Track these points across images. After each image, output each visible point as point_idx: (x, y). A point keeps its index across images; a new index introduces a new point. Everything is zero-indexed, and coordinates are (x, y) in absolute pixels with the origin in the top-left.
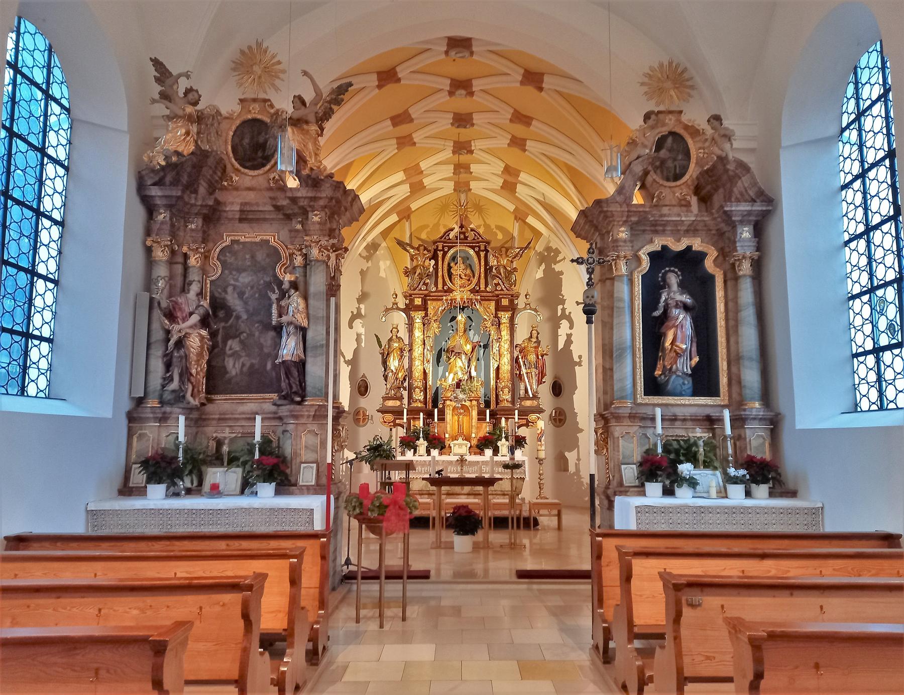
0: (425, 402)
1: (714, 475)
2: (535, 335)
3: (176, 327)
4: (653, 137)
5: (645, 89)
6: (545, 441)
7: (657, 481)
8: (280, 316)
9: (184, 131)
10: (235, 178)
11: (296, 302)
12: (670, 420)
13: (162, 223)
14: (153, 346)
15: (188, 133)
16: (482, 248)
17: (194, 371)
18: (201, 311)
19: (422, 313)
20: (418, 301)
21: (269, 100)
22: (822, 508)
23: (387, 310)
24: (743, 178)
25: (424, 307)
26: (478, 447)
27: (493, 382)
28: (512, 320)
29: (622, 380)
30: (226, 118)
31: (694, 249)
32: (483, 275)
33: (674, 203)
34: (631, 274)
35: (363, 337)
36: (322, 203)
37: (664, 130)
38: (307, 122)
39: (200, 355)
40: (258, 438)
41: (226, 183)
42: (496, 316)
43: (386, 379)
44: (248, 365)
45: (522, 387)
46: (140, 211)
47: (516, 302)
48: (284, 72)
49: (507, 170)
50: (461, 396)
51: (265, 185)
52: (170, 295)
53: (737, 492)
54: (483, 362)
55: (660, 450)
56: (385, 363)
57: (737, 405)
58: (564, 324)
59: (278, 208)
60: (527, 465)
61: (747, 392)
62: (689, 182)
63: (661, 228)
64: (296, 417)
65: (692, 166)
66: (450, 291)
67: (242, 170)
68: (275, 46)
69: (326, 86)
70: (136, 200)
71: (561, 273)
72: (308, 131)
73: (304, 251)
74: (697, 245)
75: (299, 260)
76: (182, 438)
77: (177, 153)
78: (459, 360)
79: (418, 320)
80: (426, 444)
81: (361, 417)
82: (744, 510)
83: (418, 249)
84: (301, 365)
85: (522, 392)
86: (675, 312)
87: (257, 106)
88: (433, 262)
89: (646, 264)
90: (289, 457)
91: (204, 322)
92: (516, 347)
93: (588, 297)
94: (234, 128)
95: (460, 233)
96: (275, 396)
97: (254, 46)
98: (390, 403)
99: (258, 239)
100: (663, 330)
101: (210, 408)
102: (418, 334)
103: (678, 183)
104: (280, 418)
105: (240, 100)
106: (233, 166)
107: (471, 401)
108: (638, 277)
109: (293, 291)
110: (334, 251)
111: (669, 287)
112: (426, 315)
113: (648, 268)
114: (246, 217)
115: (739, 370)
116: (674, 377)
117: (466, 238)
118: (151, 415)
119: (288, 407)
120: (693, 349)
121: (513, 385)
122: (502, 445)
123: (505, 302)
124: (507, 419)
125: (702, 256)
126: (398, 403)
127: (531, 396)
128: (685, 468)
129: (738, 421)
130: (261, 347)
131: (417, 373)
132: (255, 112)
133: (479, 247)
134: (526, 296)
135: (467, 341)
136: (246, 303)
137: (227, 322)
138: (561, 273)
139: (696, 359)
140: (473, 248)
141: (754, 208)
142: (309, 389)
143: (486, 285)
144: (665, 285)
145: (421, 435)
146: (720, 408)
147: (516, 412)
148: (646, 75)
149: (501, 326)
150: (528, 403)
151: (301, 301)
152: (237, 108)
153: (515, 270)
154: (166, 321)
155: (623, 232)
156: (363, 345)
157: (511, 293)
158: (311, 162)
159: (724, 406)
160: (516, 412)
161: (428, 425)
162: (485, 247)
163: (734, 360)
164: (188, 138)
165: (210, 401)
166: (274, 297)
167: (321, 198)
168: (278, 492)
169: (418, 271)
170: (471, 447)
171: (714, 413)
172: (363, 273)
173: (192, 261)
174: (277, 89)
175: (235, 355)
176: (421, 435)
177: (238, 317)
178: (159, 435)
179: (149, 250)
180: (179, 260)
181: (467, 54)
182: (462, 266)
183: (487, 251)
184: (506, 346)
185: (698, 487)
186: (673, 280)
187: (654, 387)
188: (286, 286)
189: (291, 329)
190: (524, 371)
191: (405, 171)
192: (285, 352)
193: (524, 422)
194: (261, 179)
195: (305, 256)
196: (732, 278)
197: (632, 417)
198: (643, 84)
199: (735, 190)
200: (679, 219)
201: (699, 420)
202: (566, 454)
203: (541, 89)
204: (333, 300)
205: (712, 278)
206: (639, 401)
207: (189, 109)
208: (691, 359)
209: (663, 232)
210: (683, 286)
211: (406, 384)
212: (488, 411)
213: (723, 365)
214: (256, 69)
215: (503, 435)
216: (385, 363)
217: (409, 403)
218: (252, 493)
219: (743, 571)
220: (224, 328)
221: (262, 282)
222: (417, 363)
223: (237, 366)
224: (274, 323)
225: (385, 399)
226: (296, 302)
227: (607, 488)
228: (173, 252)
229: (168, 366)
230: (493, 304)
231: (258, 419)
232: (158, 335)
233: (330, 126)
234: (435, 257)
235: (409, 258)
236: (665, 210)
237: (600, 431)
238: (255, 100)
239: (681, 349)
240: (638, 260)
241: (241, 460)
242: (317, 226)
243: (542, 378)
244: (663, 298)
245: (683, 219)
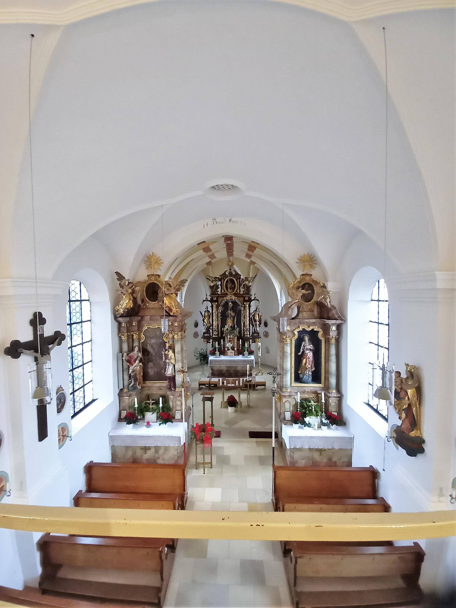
10: (147, 304)
14: (124, 371)
19: (216, 303)
23: (204, 301)
24: (333, 311)
29: (286, 382)
31: (314, 330)
33: (308, 310)
44: (156, 371)
48: (162, 263)
51: (158, 307)
56: (204, 321)
66: (227, 294)
68: (158, 251)
72: (172, 297)
86: (307, 352)
87: (153, 278)
88: (220, 283)
90: (172, 407)
92: (251, 314)
97: (151, 254)
98: (206, 335)
100: (302, 358)
103: (309, 303)
105: (147, 275)
108: (293, 341)
109: (170, 349)
111: (305, 341)
113: (297, 338)
115: (329, 375)
116: (305, 376)
120: (312, 365)
125: (318, 332)
130: (160, 365)
132: (153, 280)
133: (237, 277)
134: (255, 294)
136: (154, 349)
137: (148, 356)
139: (314, 369)
141: (337, 322)
142: (177, 385)
145: (217, 350)
148: (300, 260)
173: (135, 337)
174: (160, 270)
175: (151, 368)
176: (217, 350)
177: (152, 355)
179: (120, 338)
180: (131, 339)
186: (307, 338)
187: (298, 379)
188: (167, 348)
193: (253, 341)
194: (156, 304)
196: (328, 341)
200: (309, 321)
206: (293, 385)
216: (204, 321)
217: (213, 335)
220: (147, 358)
221: (159, 342)
223: (152, 371)
225: (204, 333)
226: (171, 353)
230: (242, 299)
234: (220, 280)
235: (212, 283)
238: (152, 275)
240: (294, 334)
245: (311, 321)
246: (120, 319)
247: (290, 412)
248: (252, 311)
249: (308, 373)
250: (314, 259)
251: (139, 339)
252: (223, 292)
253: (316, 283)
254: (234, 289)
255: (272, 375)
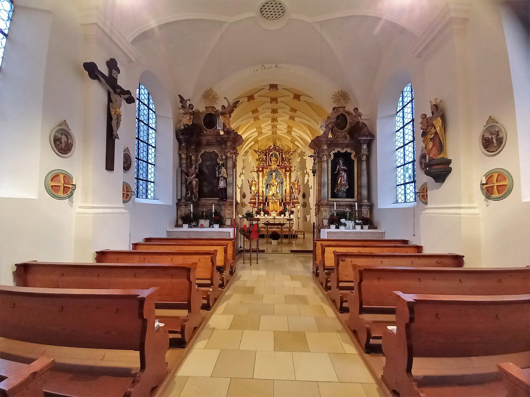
0: (263, 200)
1: (352, 222)
2: (297, 179)
3: (189, 178)
4: (335, 115)
5: (333, 100)
6: (300, 212)
7: (334, 224)
8: (219, 174)
9: (189, 118)
10: (205, 132)
11: (223, 170)
12: (338, 206)
13: (184, 146)
15: (190, 118)
16: (281, 152)
17: (195, 191)
18: (196, 173)
19: (262, 173)
20: (261, 169)
21: (214, 107)
22: (385, 232)
23: (251, 172)
25: (262, 171)
26: (279, 214)
27: (284, 194)
28: (290, 174)
29: (324, 194)
30: (202, 113)
32: (281, 161)
34: (328, 160)
35: (244, 180)
36: (231, 139)
37: (339, 113)
38: (226, 114)
39: (196, 186)
40: (213, 211)
41: (202, 134)
42: (285, 173)
43: (251, 193)
45: (293, 195)
46: (177, 143)
47: (291, 169)
48: (218, 97)
49: (289, 127)
50: (274, 199)
52: (186, 169)
53: (358, 227)
54: (281, 188)
55: (335, 215)
56: (250, 188)
57: (360, 201)
58: (307, 176)
59: (217, 141)
60: (294, 219)
61: (363, 197)
62: (347, 130)
63: (337, 145)
64: (224, 205)
65: (348, 125)
66: (271, 166)
67: (207, 129)
69: (232, 102)
70: (176, 139)
71: (306, 160)
73: (226, 154)
74: (349, 150)
75: (224, 157)
76: (192, 211)
77: (187, 125)
78: (273, 187)
79: (260, 175)
80: (263, 213)
81: (244, 205)
82: (360, 233)
83: (260, 153)
84: (225, 189)
85: (293, 197)
88: (265, 157)
89: (332, 157)
90: (223, 217)
91: (197, 177)
92: (291, 183)
93: (313, 168)
94: (204, 116)
95: (274, 147)
96: (218, 199)
97: (209, 90)
98: (252, 201)
99: (212, 151)
101: (199, 202)
102: (261, 179)
103: (343, 130)
104: (220, 205)
106: (204, 128)
107: (277, 200)
109: (222, 167)
110: (234, 154)
112: (263, 173)
114: (209, 144)
115: (361, 190)
117: (276, 149)
118: (183, 204)
119: (221, 202)
121: (290, 195)
122: (287, 213)
123: (288, 169)
124: (288, 206)
125: (350, 154)
126: (255, 201)
127: (296, 198)
128: (343, 220)
129: (360, 206)
131: (261, 191)
132: (210, 111)
133: (280, 152)
135: (276, 181)
138: (306, 160)
139: (348, 187)
140: (278, 152)
142: (228, 196)
143: (282, 164)
144: (339, 163)
145: (262, 210)
146: (354, 202)
147: (291, 203)
149: (287, 177)
150: (295, 201)
151: (225, 170)
152: (205, 110)
153: (291, 159)
154: (186, 176)
155: (325, 147)
156: (244, 183)
157: (290, 166)
158: (228, 126)
159: (356, 202)
160: (291, 203)
161: (264, 207)
162: (282, 151)
163: (360, 187)
164: (190, 120)
165: (200, 200)
166: (217, 169)
167: (231, 138)
168: (220, 227)
169: (261, 160)
170: (277, 214)
171: (353, 204)
172: (243, 160)
173: (193, 158)
176: (262, 210)
178: (185, 210)
180: (189, 158)
181: (276, 90)
182: (274, 158)
183: (282, 153)
184: (288, 183)
185: (346, 226)
186: (341, 162)
187: (334, 195)
188: (220, 165)
189: (222, 178)
190: (294, 191)
191: (256, 128)
192: (221, 185)
193: (294, 206)
195: (226, 156)
196: (360, 161)
197: (327, 205)
198: (332, 98)
199: (362, 132)
201: (347, 206)
202: (307, 216)
203: (300, 100)
204: (234, 169)
205: (353, 161)
207: (190, 111)
208: (346, 187)
209: (338, 147)
210: (344, 164)
211: (257, 195)
212: (282, 203)
213: (356, 189)
214: (210, 97)
215: (287, 210)
216: (250, 188)
217: (258, 201)
218: (212, 227)
219: (359, 251)
222: (260, 188)
224: (217, 176)
227: (319, 226)
228: (187, 156)
229: (187, 190)
230: (284, 169)
231: (213, 205)
232: (184, 181)
233: (233, 115)
234: (266, 155)
236: (339, 139)
237: (317, 209)
239: (343, 184)
240: (330, 155)
241: (209, 217)
242: (229, 146)
243: (299, 193)
244: (338, 168)
246: (181, 137)
247: (327, 220)
248: (292, 181)
249: (342, 190)
250: (347, 95)
251: (196, 161)
252: (267, 164)
253: (349, 113)
254: (277, 162)
255: (313, 158)
